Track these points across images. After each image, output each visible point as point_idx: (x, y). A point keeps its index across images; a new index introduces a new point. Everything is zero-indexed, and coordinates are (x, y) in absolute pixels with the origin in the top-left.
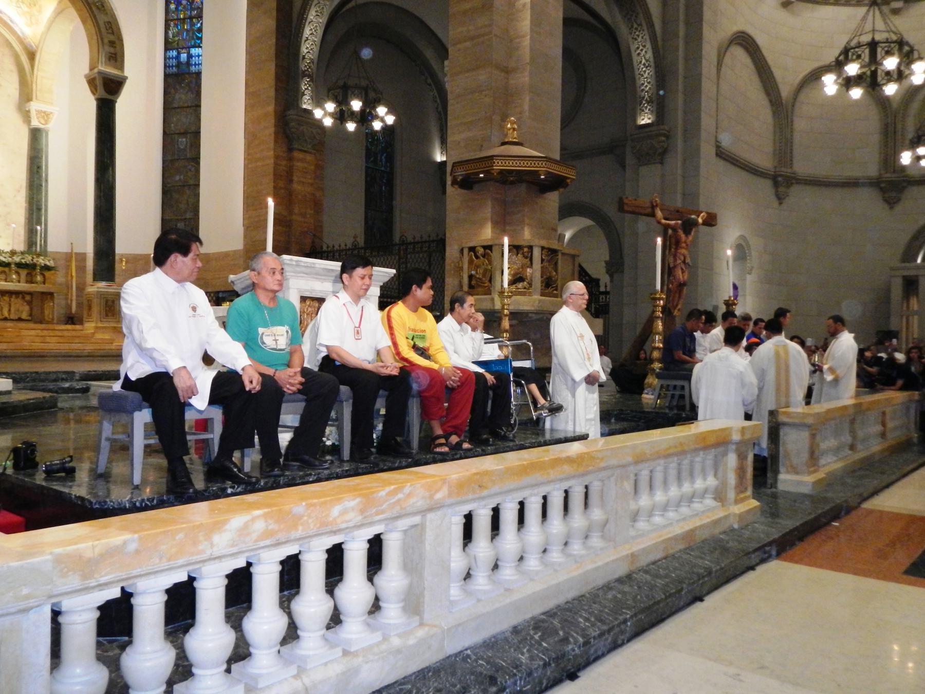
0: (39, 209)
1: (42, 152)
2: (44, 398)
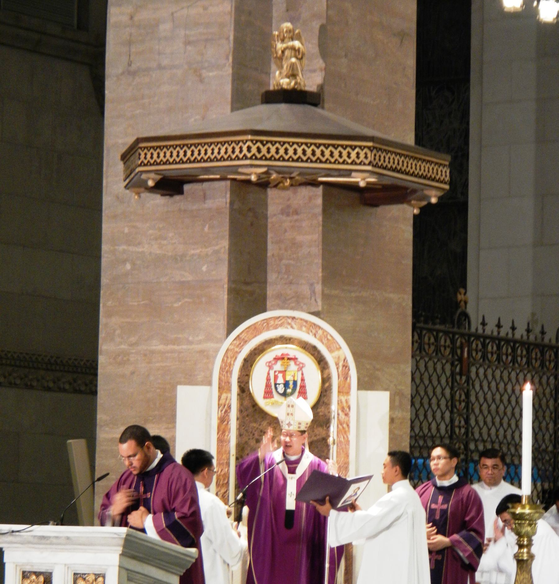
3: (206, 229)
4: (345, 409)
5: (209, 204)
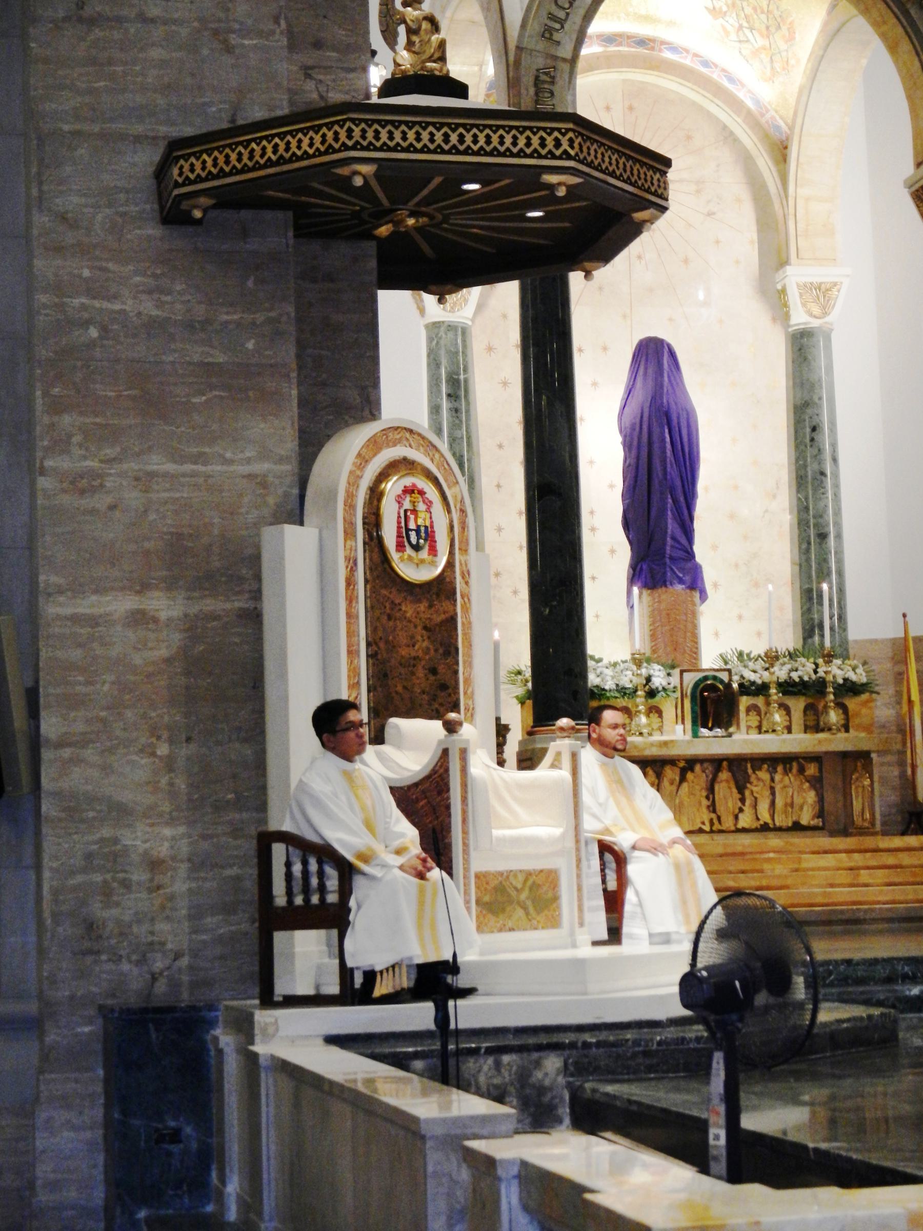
0: (823, 537)
1: (821, 388)
2: (870, 1017)
3: (250, 283)
4: (466, 575)
5: (253, 244)
